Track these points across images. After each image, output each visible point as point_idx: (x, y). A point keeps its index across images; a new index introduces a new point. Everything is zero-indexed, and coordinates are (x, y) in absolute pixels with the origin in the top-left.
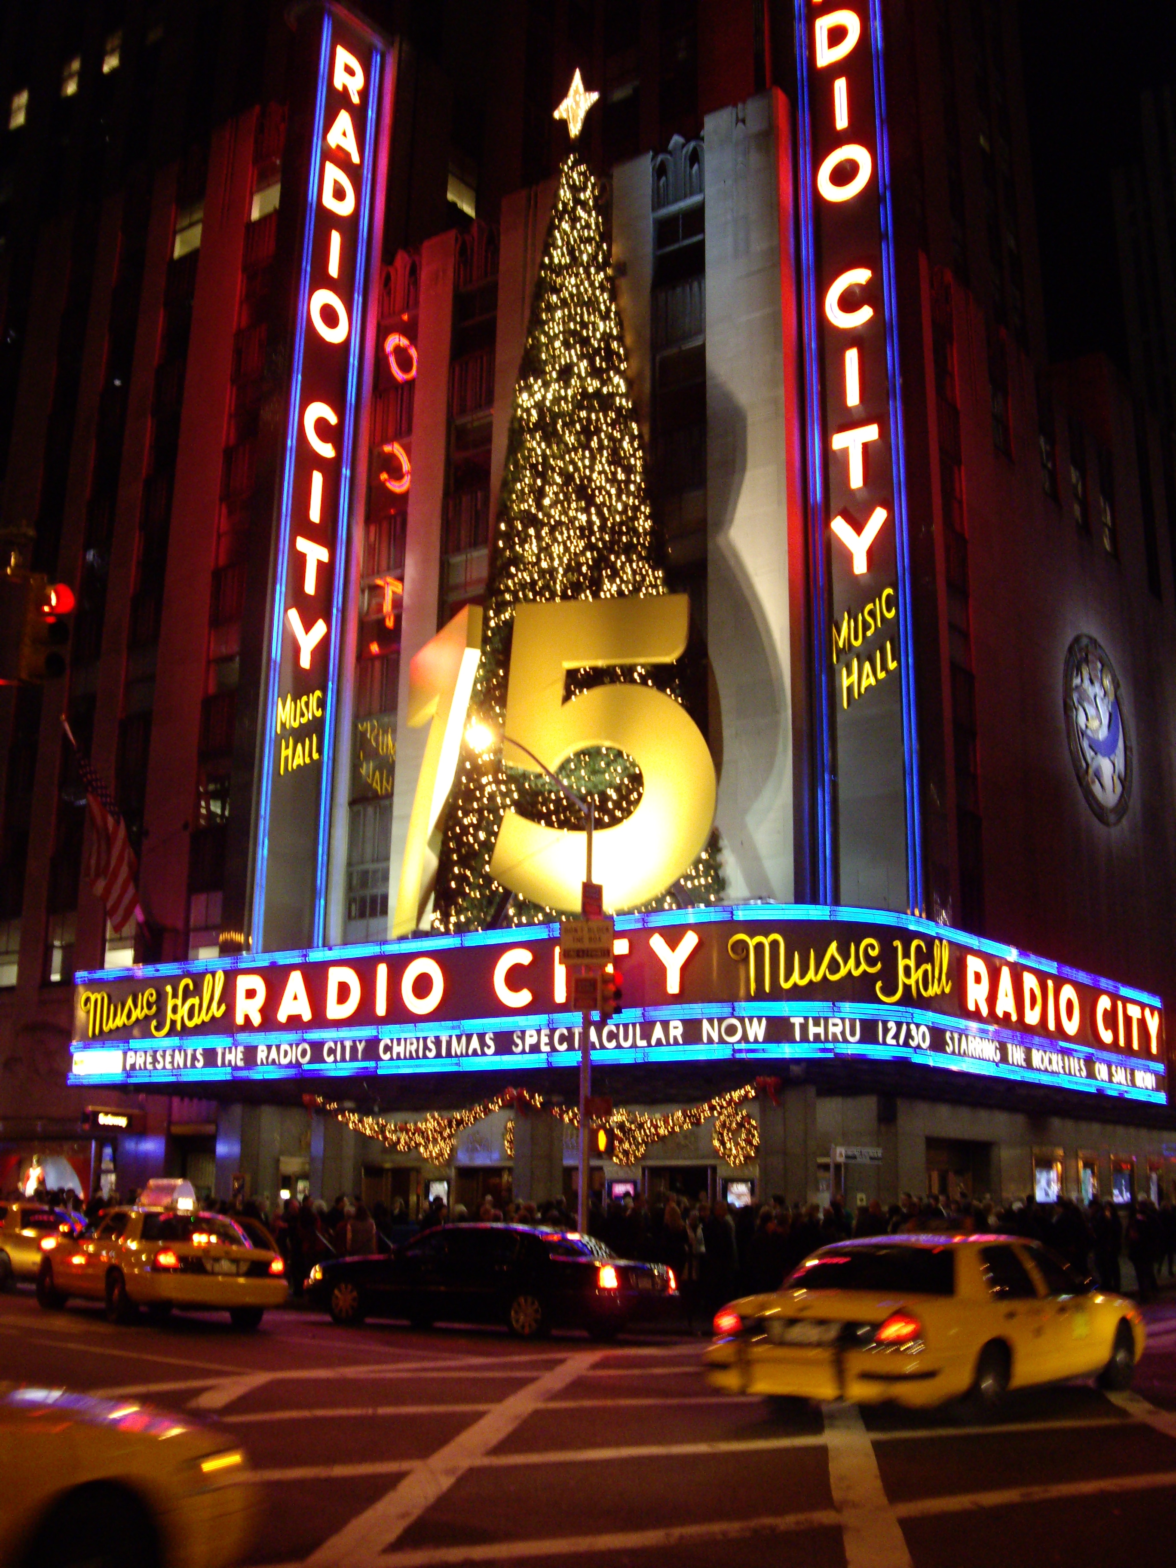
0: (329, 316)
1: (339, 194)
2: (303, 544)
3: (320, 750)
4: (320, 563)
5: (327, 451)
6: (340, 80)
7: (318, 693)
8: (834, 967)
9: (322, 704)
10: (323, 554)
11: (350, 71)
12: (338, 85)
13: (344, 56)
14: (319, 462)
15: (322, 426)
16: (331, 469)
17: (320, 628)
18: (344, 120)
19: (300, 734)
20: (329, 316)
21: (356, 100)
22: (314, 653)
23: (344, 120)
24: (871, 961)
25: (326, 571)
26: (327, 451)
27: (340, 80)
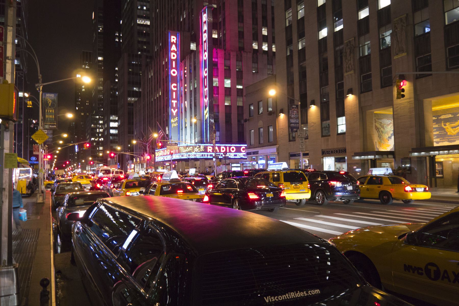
0: (174, 73)
1: (174, 56)
2: (173, 101)
3: (178, 124)
4: (175, 103)
5: (175, 89)
6: (172, 40)
7: (177, 117)
8: (187, 150)
9: (177, 119)
10: (176, 101)
11: (174, 39)
12: (172, 41)
13: (172, 37)
15: (174, 87)
16: (176, 91)
17: (176, 110)
18: (174, 46)
19: (175, 123)
20: (174, 73)
21: (175, 42)
22: (176, 113)
23: (174, 46)
24: (191, 149)
25: (176, 104)
26: (175, 89)
27: (172, 40)
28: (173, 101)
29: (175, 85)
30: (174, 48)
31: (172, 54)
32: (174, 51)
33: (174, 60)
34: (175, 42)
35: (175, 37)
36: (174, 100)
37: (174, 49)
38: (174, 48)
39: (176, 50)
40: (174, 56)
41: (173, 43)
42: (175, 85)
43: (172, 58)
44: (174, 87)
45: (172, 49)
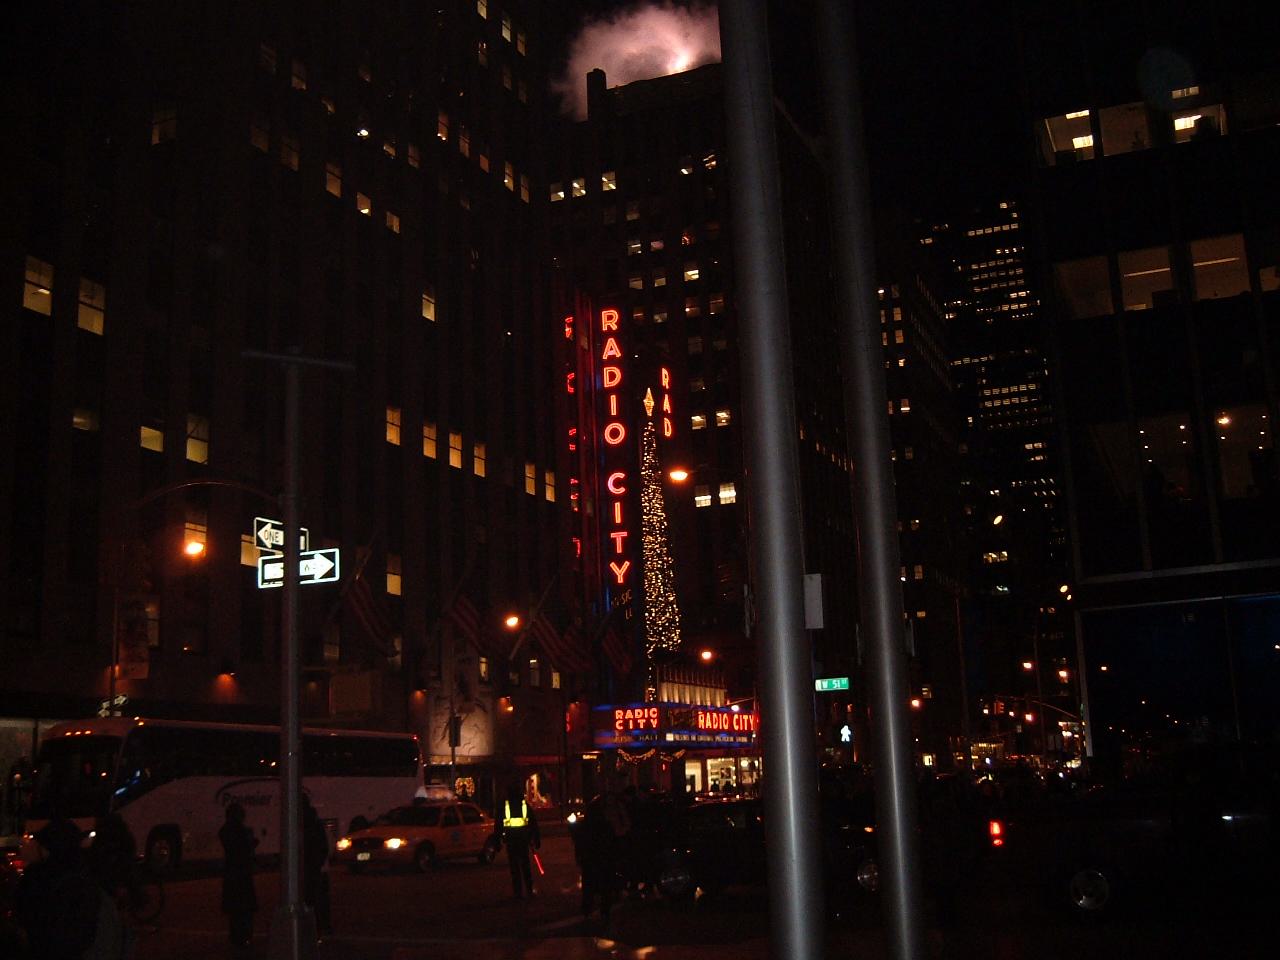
1: (612, 376)
2: (613, 535)
14: (617, 498)
15: (617, 483)
18: (611, 342)
21: (614, 327)
23: (611, 342)
28: (613, 535)
29: (621, 475)
30: (612, 349)
31: (607, 370)
32: (612, 361)
33: (612, 390)
34: (614, 327)
35: (615, 313)
36: (619, 528)
37: (611, 353)
38: (612, 349)
39: (619, 355)
40: (612, 376)
41: (610, 333)
42: (621, 475)
43: (607, 383)
44: (617, 483)
45: (605, 357)
